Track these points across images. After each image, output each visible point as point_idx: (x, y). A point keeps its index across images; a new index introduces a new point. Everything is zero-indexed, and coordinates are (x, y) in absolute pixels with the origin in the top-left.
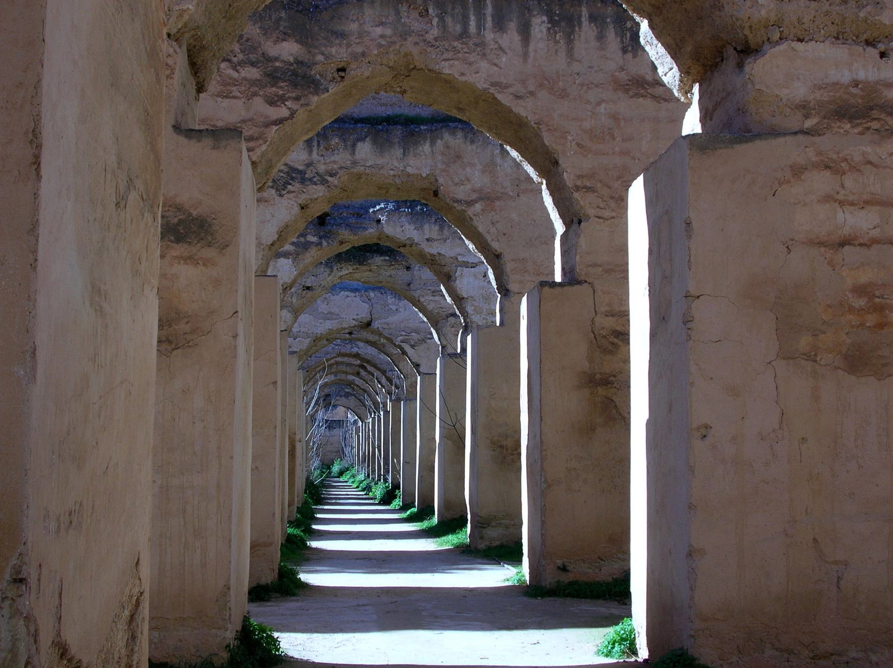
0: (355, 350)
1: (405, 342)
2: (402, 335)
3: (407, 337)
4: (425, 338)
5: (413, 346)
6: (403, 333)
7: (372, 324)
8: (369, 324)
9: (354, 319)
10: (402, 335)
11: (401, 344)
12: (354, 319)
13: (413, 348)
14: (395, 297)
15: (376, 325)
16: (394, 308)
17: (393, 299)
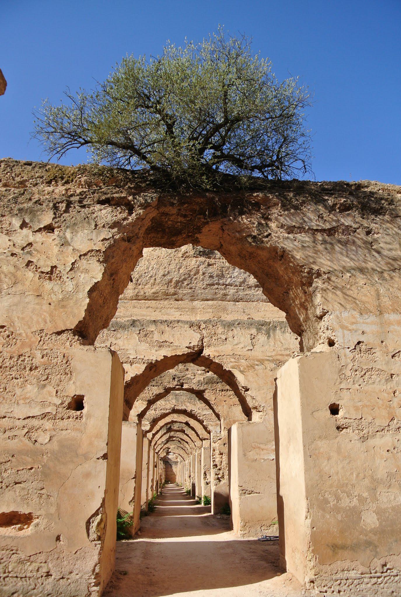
0: (183, 408)
1: (235, 368)
2: (231, 362)
3: (237, 364)
4: (254, 364)
5: (241, 372)
6: (233, 360)
7: (204, 352)
8: (201, 351)
9: (187, 347)
10: (231, 362)
11: (230, 369)
12: (187, 347)
13: (243, 374)
14: (224, 328)
15: (206, 352)
16: (224, 337)
17: (223, 330)
